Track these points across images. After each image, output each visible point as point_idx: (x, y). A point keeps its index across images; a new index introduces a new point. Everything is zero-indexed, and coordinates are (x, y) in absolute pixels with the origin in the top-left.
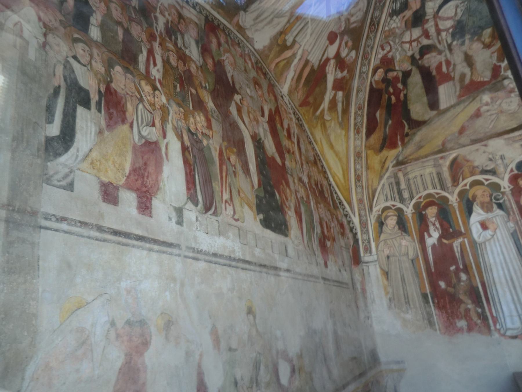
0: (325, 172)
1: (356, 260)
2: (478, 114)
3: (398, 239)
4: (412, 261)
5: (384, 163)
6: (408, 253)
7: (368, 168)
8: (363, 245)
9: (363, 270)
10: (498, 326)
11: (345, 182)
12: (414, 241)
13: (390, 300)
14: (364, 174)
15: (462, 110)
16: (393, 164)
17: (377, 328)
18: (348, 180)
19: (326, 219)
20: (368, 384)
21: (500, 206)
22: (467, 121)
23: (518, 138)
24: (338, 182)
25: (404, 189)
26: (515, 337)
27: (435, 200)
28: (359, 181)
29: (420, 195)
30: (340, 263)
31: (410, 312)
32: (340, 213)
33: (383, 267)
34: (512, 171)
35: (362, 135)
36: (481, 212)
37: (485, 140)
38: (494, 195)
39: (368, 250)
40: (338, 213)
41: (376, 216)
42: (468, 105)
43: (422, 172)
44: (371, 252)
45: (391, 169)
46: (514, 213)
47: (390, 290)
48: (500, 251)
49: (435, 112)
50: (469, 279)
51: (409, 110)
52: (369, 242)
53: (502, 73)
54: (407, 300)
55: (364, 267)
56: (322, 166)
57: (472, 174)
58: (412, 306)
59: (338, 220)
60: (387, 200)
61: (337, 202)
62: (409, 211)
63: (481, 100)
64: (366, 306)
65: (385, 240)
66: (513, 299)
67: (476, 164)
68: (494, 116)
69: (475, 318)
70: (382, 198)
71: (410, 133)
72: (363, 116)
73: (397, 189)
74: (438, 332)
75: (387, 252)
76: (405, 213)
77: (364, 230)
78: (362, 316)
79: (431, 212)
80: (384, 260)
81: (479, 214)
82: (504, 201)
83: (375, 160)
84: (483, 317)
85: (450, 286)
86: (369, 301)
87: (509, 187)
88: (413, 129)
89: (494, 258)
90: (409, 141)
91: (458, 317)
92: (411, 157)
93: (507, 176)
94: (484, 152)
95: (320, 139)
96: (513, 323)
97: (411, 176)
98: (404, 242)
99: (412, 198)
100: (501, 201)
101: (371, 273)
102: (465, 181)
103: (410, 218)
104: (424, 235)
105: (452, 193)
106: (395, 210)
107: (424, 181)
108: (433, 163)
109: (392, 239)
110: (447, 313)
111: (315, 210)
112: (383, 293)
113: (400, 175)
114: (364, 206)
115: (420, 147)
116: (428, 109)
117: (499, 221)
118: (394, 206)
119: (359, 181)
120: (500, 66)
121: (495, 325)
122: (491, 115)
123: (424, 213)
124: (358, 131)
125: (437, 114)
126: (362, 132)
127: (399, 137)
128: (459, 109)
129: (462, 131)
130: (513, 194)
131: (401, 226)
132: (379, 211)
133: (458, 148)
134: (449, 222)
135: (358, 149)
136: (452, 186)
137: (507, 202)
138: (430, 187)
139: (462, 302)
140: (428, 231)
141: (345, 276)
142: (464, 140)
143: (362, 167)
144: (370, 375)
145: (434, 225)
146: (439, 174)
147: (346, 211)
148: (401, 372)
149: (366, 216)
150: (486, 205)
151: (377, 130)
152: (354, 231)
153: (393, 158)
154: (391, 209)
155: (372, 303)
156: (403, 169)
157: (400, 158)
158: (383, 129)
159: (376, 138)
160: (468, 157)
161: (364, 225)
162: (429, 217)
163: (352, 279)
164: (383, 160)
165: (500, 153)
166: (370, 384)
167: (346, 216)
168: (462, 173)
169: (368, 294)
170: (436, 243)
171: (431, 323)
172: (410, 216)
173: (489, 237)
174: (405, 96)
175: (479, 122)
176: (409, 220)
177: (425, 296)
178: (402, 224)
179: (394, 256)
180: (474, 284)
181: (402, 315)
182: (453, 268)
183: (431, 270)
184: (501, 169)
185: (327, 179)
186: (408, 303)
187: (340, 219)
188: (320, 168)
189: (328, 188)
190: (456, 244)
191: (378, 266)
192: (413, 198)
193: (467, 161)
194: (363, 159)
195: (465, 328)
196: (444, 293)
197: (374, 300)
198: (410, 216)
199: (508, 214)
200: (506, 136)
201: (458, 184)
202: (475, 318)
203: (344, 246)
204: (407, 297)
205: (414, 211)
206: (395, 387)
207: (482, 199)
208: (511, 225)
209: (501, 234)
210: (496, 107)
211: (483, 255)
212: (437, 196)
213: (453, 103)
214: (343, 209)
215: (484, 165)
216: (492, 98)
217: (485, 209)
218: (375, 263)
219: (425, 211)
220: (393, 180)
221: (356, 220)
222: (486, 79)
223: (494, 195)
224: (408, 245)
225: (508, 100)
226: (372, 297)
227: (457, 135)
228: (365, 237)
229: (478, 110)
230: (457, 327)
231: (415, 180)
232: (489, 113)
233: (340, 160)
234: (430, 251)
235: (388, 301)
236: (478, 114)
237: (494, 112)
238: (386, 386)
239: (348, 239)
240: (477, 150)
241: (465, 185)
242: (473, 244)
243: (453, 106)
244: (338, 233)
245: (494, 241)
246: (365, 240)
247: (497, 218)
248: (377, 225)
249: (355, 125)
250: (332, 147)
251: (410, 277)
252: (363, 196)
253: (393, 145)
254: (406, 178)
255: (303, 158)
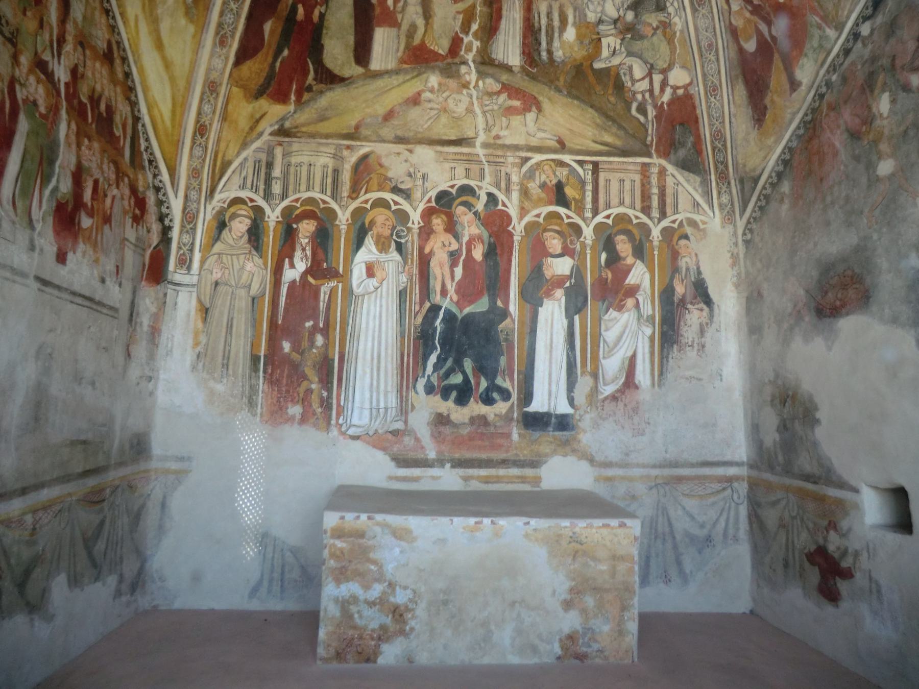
0: (132, 89)
1: (156, 271)
2: (415, 100)
3: (242, 257)
4: (253, 299)
5: (258, 121)
6: (250, 285)
7: (224, 118)
8: (178, 253)
9: (165, 295)
10: (341, 421)
11: (173, 127)
12: (266, 269)
13: (198, 356)
14: (216, 126)
15: (399, 85)
16: (272, 129)
17: (162, 398)
18: (180, 126)
19: (97, 174)
20: (103, 490)
21: (400, 248)
22: (400, 104)
23: (451, 157)
24: (159, 120)
25: (277, 178)
26: (355, 438)
27: (317, 211)
28: (202, 136)
29: (297, 196)
30: (110, 267)
31: (225, 380)
32: (145, 179)
33: (202, 298)
34: (429, 201)
35: (228, 52)
36: (374, 249)
37: (412, 143)
38: (398, 228)
39: (185, 262)
40: (140, 177)
41: (217, 209)
42: (408, 80)
43: (312, 160)
44: (189, 268)
45: (266, 137)
46: (412, 262)
47: (203, 339)
48: (378, 314)
49: (360, 70)
50: (326, 346)
51: (322, 46)
52: (191, 250)
53: (462, 53)
54: (225, 361)
55: (170, 292)
56: (128, 75)
57: (381, 188)
58: (230, 372)
59: (134, 190)
60: (243, 187)
61: (145, 157)
62: (273, 216)
63: (426, 81)
64: (152, 357)
65: (219, 254)
66: (372, 385)
67: (390, 174)
68: (434, 112)
69: (315, 405)
70: (237, 180)
71: (314, 88)
72: (238, 15)
73: (266, 173)
74: (258, 419)
75: (217, 275)
76: (266, 219)
77: (188, 227)
78: (134, 372)
79: (306, 228)
80: (208, 289)
81: (370, 251)
82: (407, 241)
83: (244, 110)
84: (326, 405)
85: (298, 353)
86: (161, 351)
87: (419, 223)
88: (321, 82)
89: (367, 323)
90: (309, 101)
91: (292, 401)
92: (304, 129)
93: (422, 207)
94: (406, 161)
95: (136, 16)
96: (360, 419)
97: (294, 160)
98: (249, 266)
99: (284, 196)
100: (403, 241)
101: (179, 304)
102: (368, 196)
103: (272, 228)
104: (283, 261)
105: (344, 208)
106: (252, 207)
107: (312, 176)
108: (333, 151)
109: (232, 255)
110: (279, 391)
111: (69, 145)
112: (190, 342)
113: (278, 151)
114: (200, 184)
115: (322, 119)
116: (352, 59)
117: (391, 268)
118: (252, 200)
119: (202, 136)
120: (462, 40)
121: (338, 419)
122: (431, 109)
123: (295, 226)
124: (222, 41)
125: (363, 74)
126: (230, 46)
127: (294, 87)
128: (395, 80)
129: (389, 116)
130: (420, 235)
131: (253, 238)
132: (224, 202)
133: (375, 141)
134: (326, 252)
135: (214, 76)
136: (349, 197)
137: (409, 244)
138: (317, 188)
139: (305, 377)
140: (291, 258)
141: (116, 295)
142: (387, 132)
143: (214, 112)
144: (113, 476)
145: (304, 250)
146: (336, 172)
147: (161, 181)
148: (181, 475)
149: (199, 203)
150: (383, 240)
151: (260, 56)
152: (167, 222)
153: (275, 119)
154: (246, 204)
155: (167, 354)
156: (285, 144)
157: (287, 124)
158: (270, 59)
159: (255, 68)
160: (384, 161)
161: (189, 218)
162: (300, 235)
163: (133, 304)
164: (258, 116)
165: (424, 170)
166: (108, 491)
167: (157, 189)
168: (368, 182)
169: (163, 339)
170: (298, 280)
171: (251, 404)
172: (272, 225)
173: (372, 289)
174: (322, 16)
175: (414, 113)
176: (269, 231)
177: (255, 359)
178: (255, 234)
179: (226, 284)
180: (330, 356)
181: (212, 384)
182: (309, 324)
183: (277, 321)
184: (418, 194)
185: (134, 104)
186: (226, 366)
187: (141, 189)
188: (120, 76)
189: (130, 121)
190: (325, 289)
191: (194, 295)
192: (287, 197)
193: (381, 165)
194: (221, 99)
195: (298, 417)
196: (286, 359)
197: (171, 351)
198: (272, 225)
199: (405, 262)
200: (439, 148)
201: (357, 198)
202: (315, 405)
203: (133, 240)
204: (226, 357)
205: (280, 219)
206: (165, 497)
207: (380, 230)
208: (404, 278)
209: (388, 289)
210: (441, 99)
211: (355, 312)
212: (322, 206)
213: (389, 67)
214: (155, 176)
215: (400, 180)
216: (440, 84)
217: (380, 247)
218: (191, 289)
219: (297, 223)
220: (263, 157)
221: (176, 205)
222: (441, 52)
223: (398, 228)
224: (253, 271)
225: (457, 97)
226: (169, 345)
227: (380, 119)
228: (186, 238)
229: (419, 94)
230: (287, 414)
231: (298, 168)
232: (430, 105)
233: (172, 79)
234: (284, 290)
235: (195, 357)
236: (415, 100)
237: (436, 106)
238: (149, 495)
239: (149, 231)
240: (399, 154)
241: (366, 202)
242: (348, 292)
243: (387, 72)
244: (125, 213)
245: (376, 296)
246: (184, 245)
247: (390, 263)
248: (215, 224)
249: (220, 25)
250: (159, 45)
251: (242, 325)
252: (203, 167)
253: (281, 97)
254: (285, 161)
255: (70, 27)
